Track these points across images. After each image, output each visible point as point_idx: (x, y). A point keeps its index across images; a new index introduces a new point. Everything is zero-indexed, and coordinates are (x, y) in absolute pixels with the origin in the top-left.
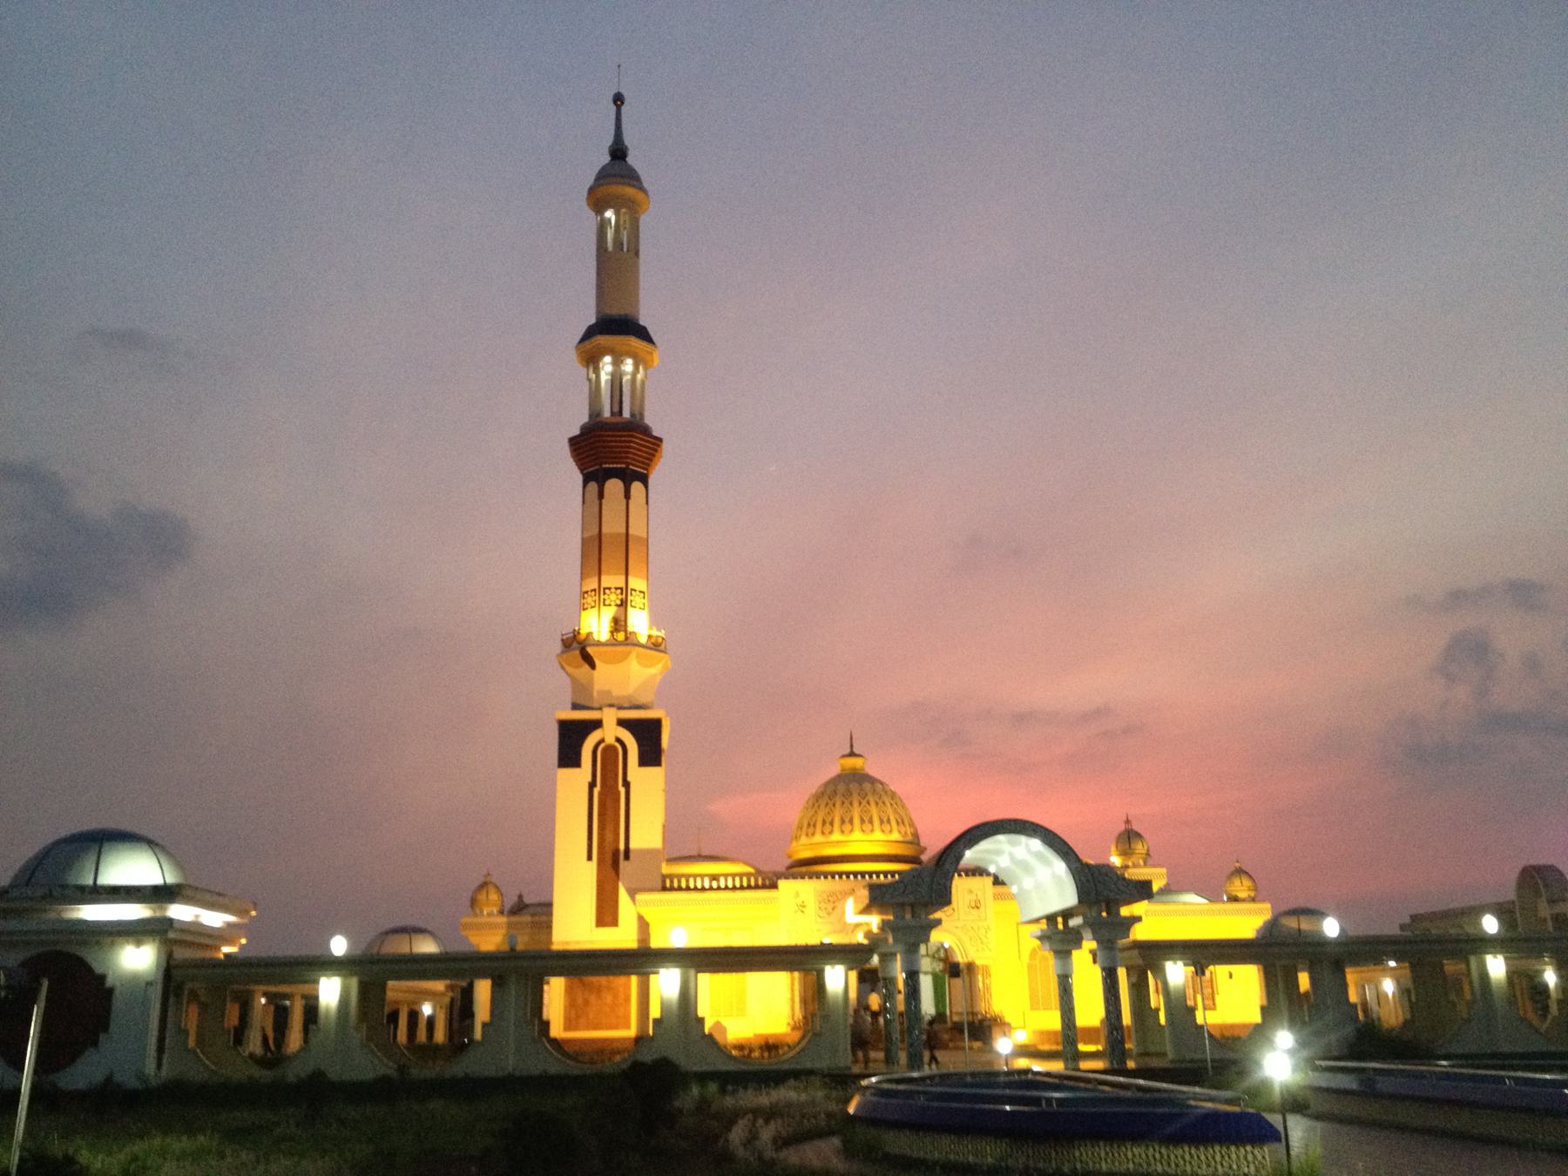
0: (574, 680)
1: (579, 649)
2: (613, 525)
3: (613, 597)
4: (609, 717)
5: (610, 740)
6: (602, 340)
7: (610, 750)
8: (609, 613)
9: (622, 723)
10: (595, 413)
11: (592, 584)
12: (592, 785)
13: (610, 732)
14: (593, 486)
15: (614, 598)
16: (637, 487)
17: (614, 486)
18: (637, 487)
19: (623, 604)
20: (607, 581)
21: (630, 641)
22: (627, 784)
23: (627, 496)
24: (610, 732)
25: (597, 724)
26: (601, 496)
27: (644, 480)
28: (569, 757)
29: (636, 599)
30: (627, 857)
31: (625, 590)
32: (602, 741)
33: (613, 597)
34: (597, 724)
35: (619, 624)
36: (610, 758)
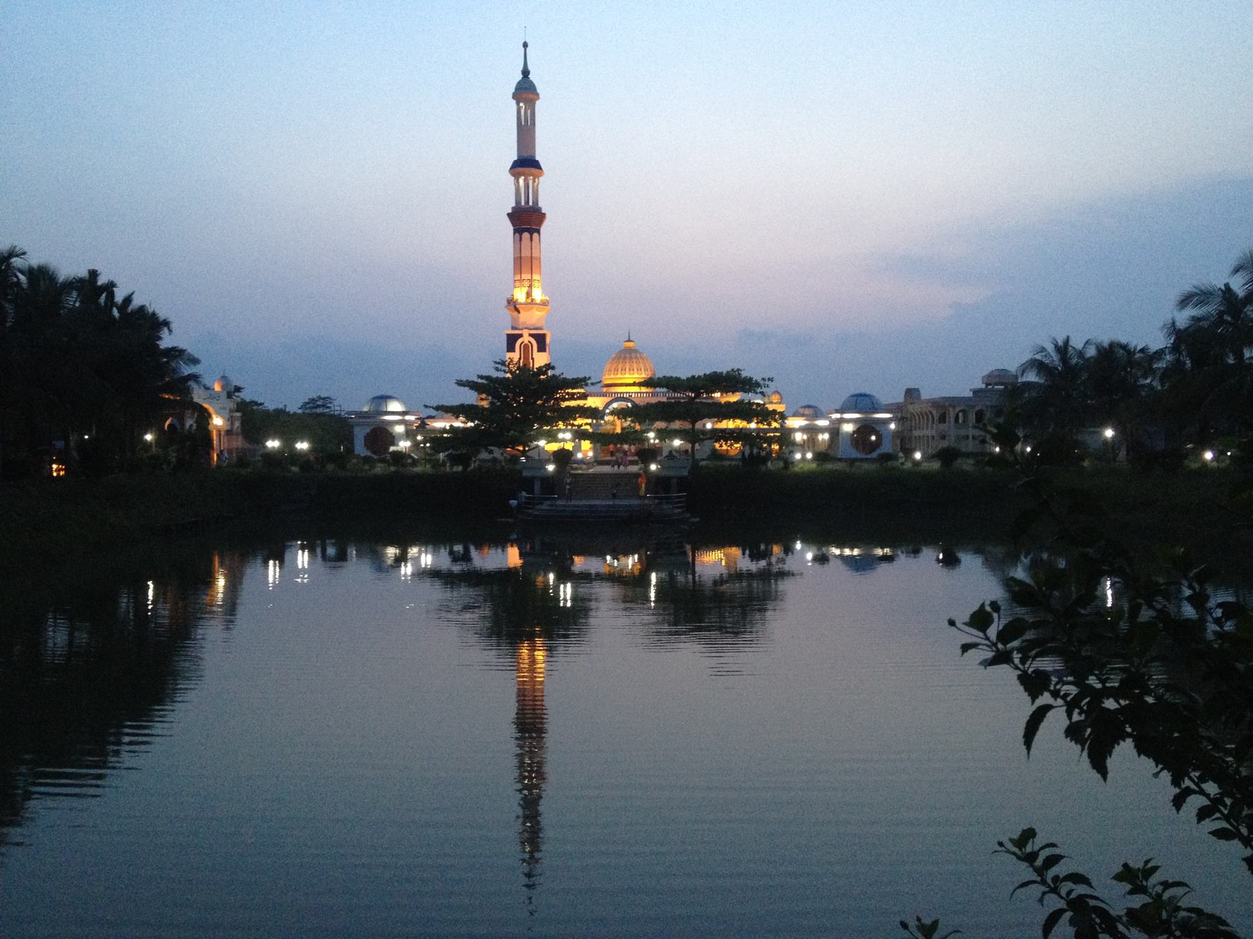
0: (513, 318)
1: (513, 305)
2: (526, 253)
4: (526, 333)
6: (520, 169)
7: (526, 347)
8: (525, 290)
9: (531, 335)
10: (518, 202)
11: (518, 277)
13: (526, 338)
15: (527, 284)
17: (526, 235)
18: (535, 235)
19: (530, 286)
20: (524, 276)
21: (533, 302)
24: (526, 338)
25: (521, 336)
27: (538, 231)
29: (536, 284)
31: (531, 280)
34: (521, 336)
35: (529, 294)
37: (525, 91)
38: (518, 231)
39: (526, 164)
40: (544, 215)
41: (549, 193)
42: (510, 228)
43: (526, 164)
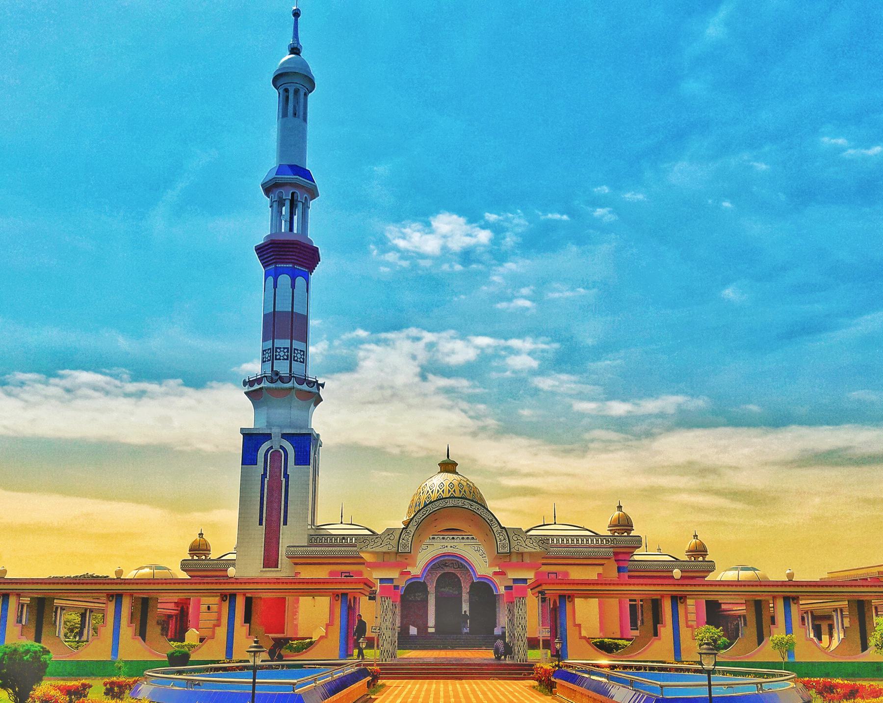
2: (284, 306)
5: (276, 447)
9: (285, 436)
12: (264, 476)
14: (271, 279)
16: (300, 281)
18: (300, 281)
22: (287, 476)
23: (293, 286)
25: (268, 437)
26: (275, 286)
28: (249, 458)
30: (285, 523)
32: (271, 448)
33: (282, 354)
34: (268, 437)
36: (275, 456)
38: (273, 274)
40: (316, 250)
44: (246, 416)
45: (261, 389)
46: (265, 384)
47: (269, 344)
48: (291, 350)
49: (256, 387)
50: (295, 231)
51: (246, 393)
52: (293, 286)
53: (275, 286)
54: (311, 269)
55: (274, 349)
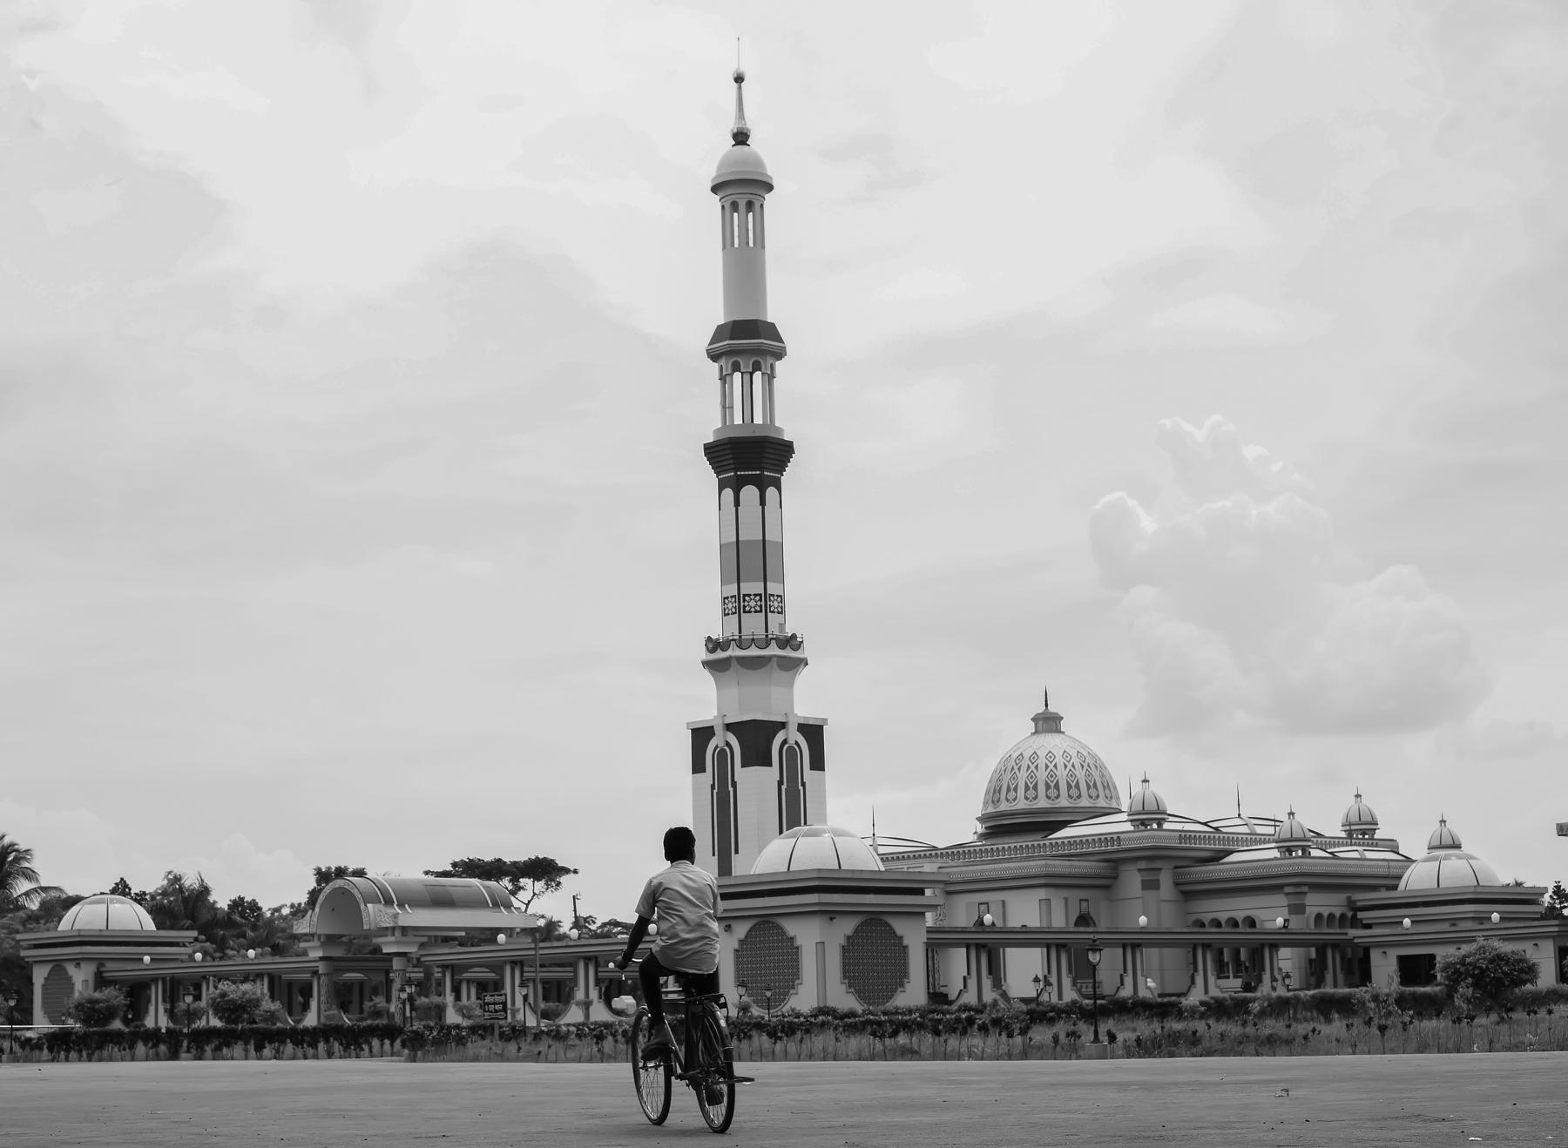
2: (751, 533)
3: (752, 603)
14: (728, 493)
17: (750, 493)
18: (771, 492)
23: (763, 502)
26: (737, 503)
33: (752, 603)
37: (743, 191)
39: (747, 344)
41: (795, 402)
42: (708, 477)
43: (747, 344)
44: (706, 701)
45: (729, 659)
46: (734, 652)
47: (732, 590)
48: (765, 596)
49: (720, 655)
50: (758, 420)
51: (706, 664)
52: (763, 502)
53: (737, 503)
54: (781, 470)
55: (740, 598)
